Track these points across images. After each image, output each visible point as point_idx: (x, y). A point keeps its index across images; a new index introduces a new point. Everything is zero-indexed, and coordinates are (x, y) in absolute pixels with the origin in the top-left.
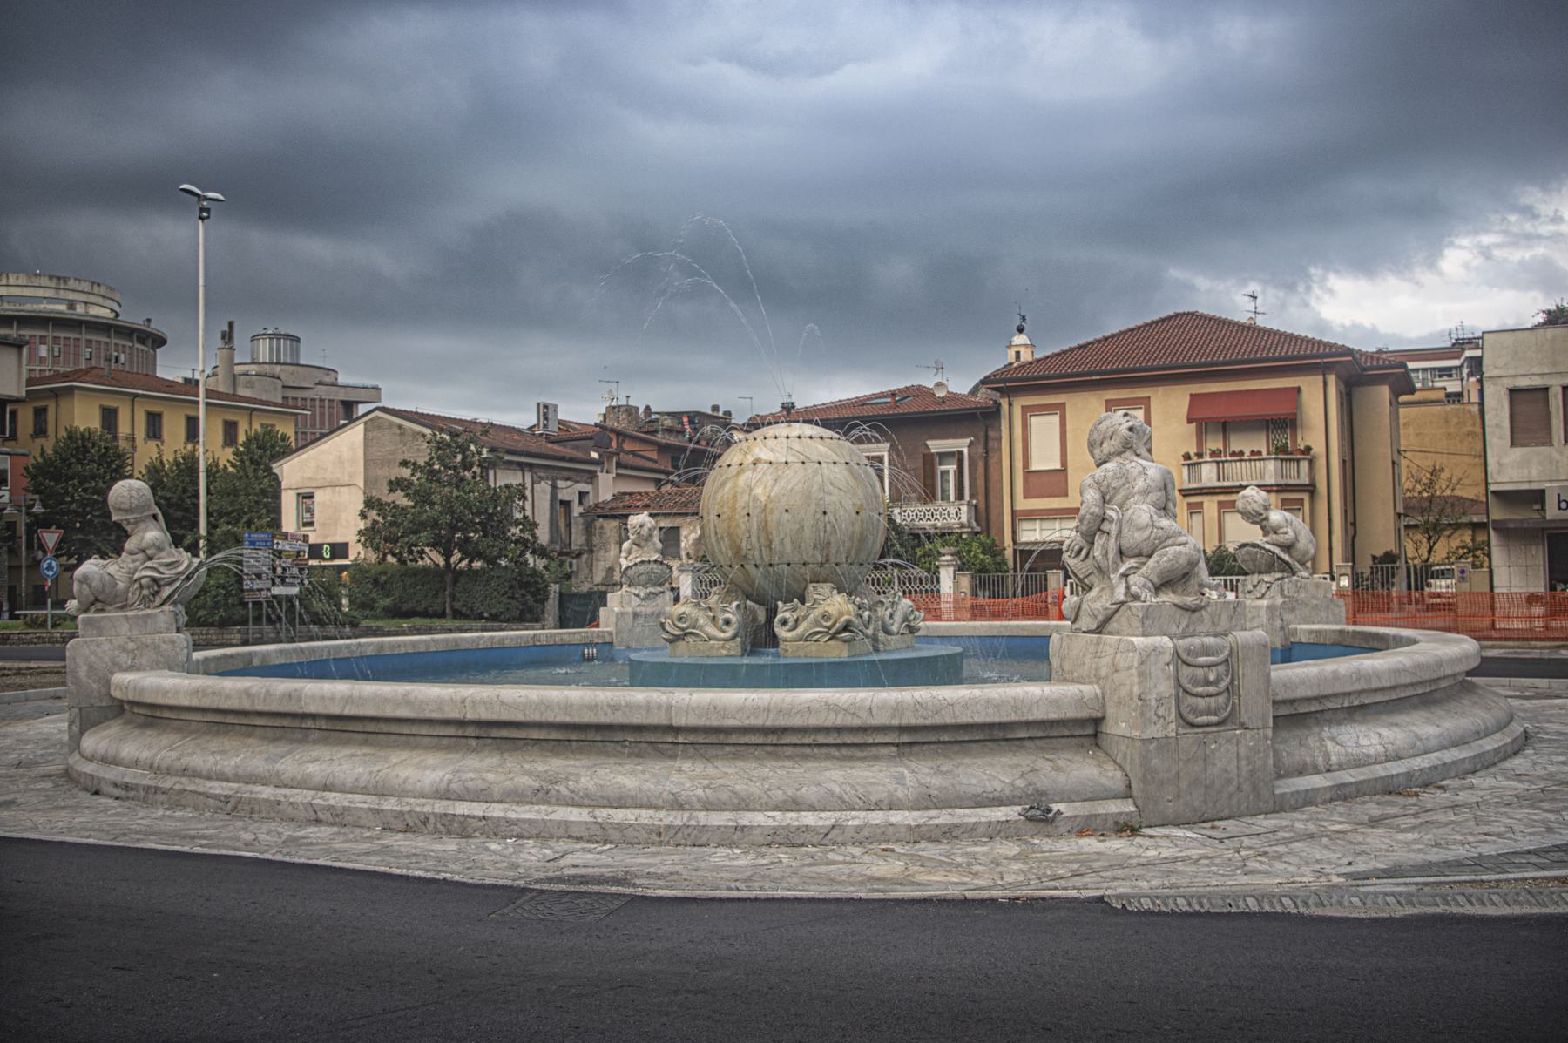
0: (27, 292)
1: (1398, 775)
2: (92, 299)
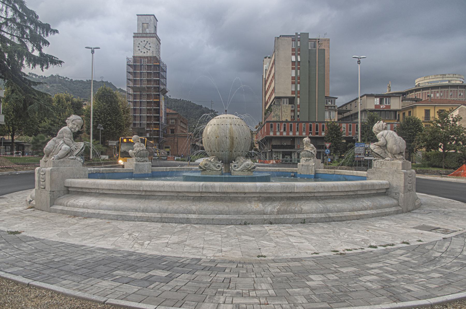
0: (434, 80)
1: (79, 212)
2: (453, 79)
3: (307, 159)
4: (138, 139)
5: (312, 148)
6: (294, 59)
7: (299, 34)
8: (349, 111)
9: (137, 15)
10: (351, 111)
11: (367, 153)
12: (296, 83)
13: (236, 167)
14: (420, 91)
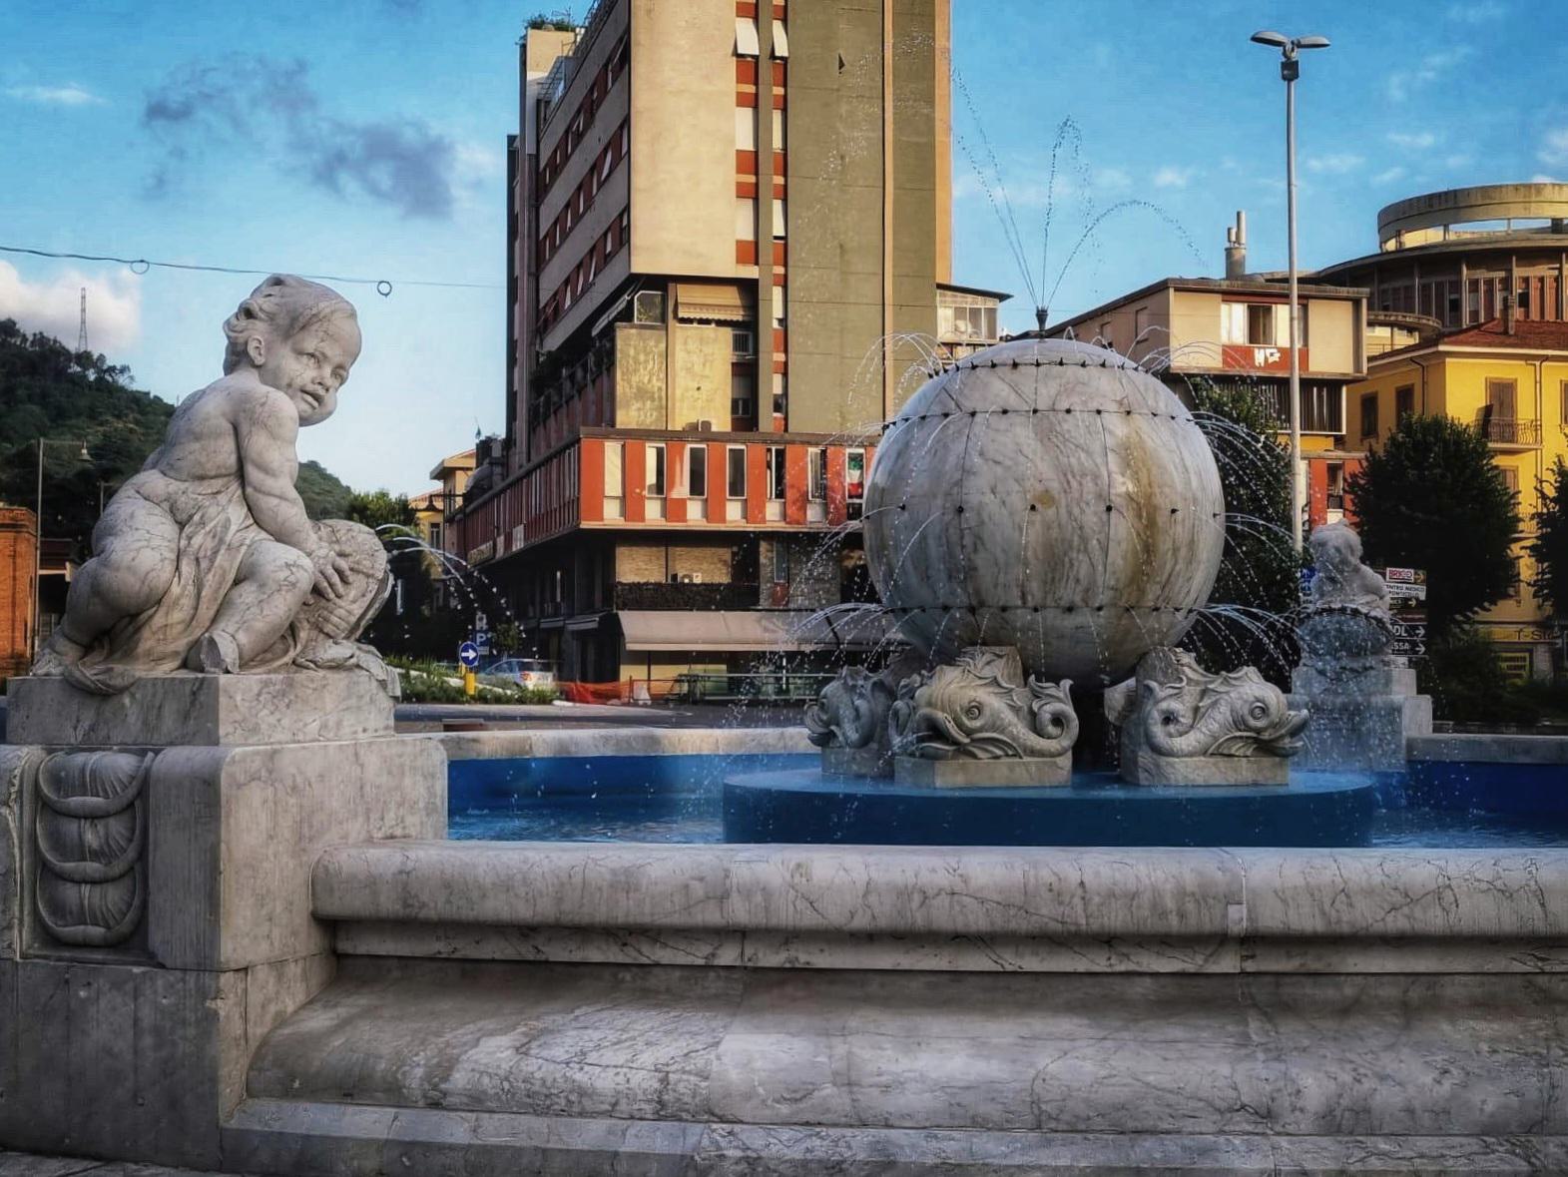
13: (1172, 728)
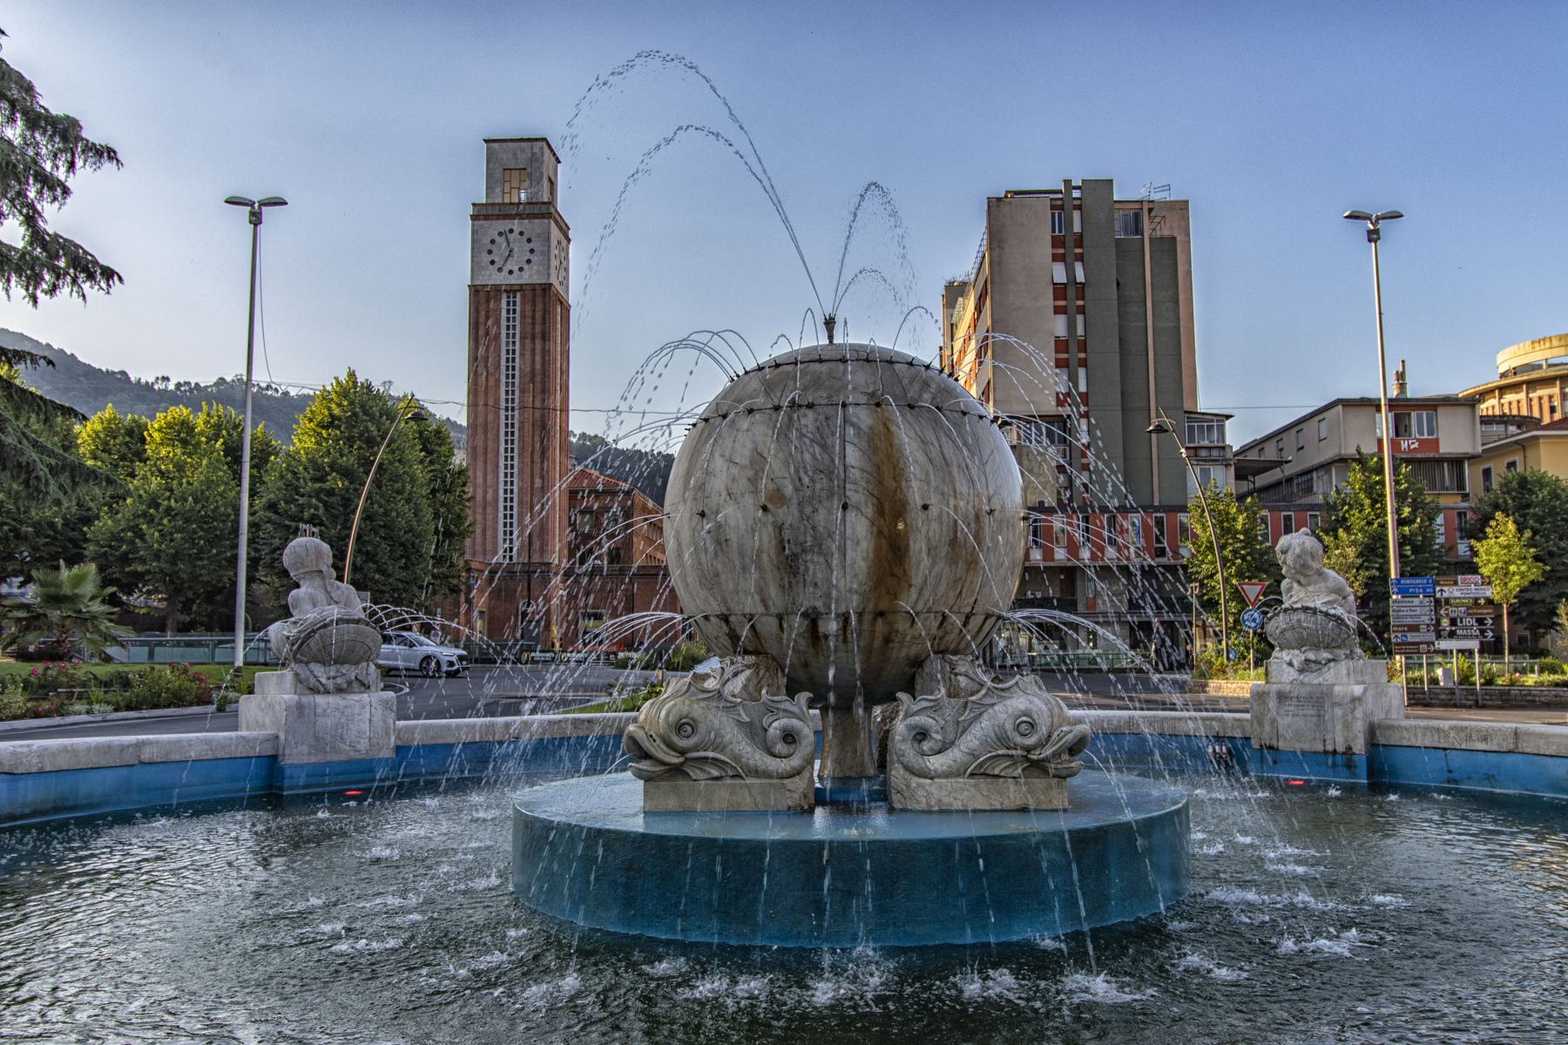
3: (1307, 661)
4: (319, 554)
5: (1338, 591)
6: (1060, 274)
7: (1077, 182)
8: (1280, 463)
9: (486, 141)
10: (1286, 466)
11: (1445, 622)
12: (1074, 363)
13: (926, 746)
14: (1554, 385)
